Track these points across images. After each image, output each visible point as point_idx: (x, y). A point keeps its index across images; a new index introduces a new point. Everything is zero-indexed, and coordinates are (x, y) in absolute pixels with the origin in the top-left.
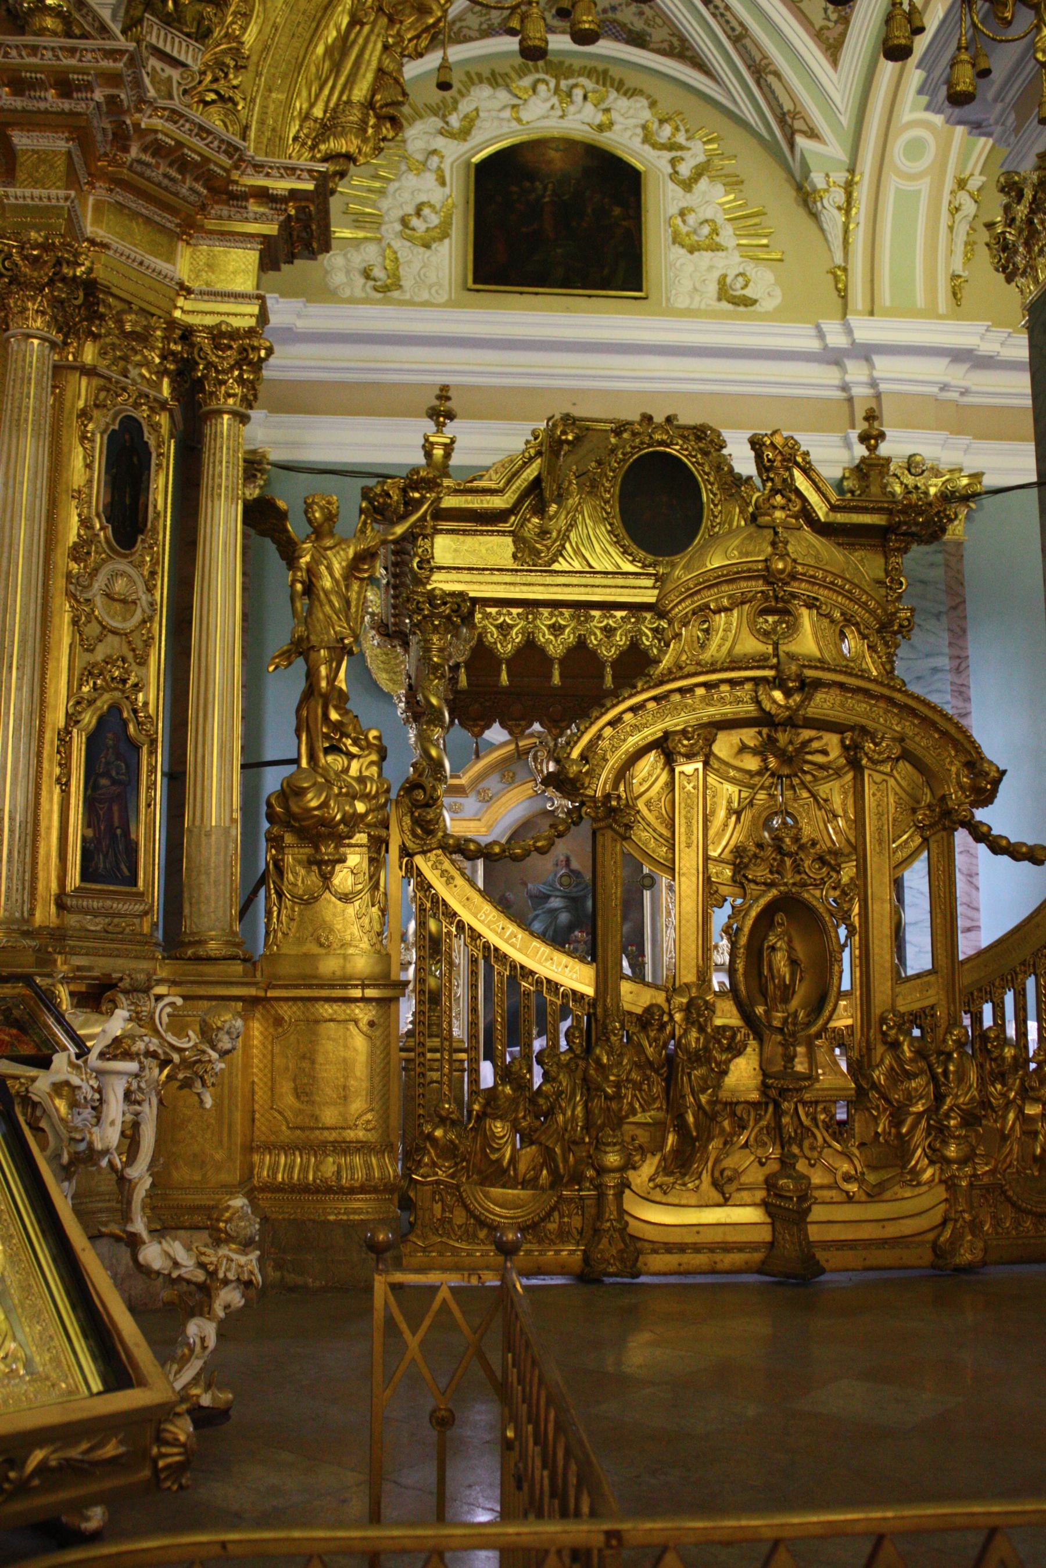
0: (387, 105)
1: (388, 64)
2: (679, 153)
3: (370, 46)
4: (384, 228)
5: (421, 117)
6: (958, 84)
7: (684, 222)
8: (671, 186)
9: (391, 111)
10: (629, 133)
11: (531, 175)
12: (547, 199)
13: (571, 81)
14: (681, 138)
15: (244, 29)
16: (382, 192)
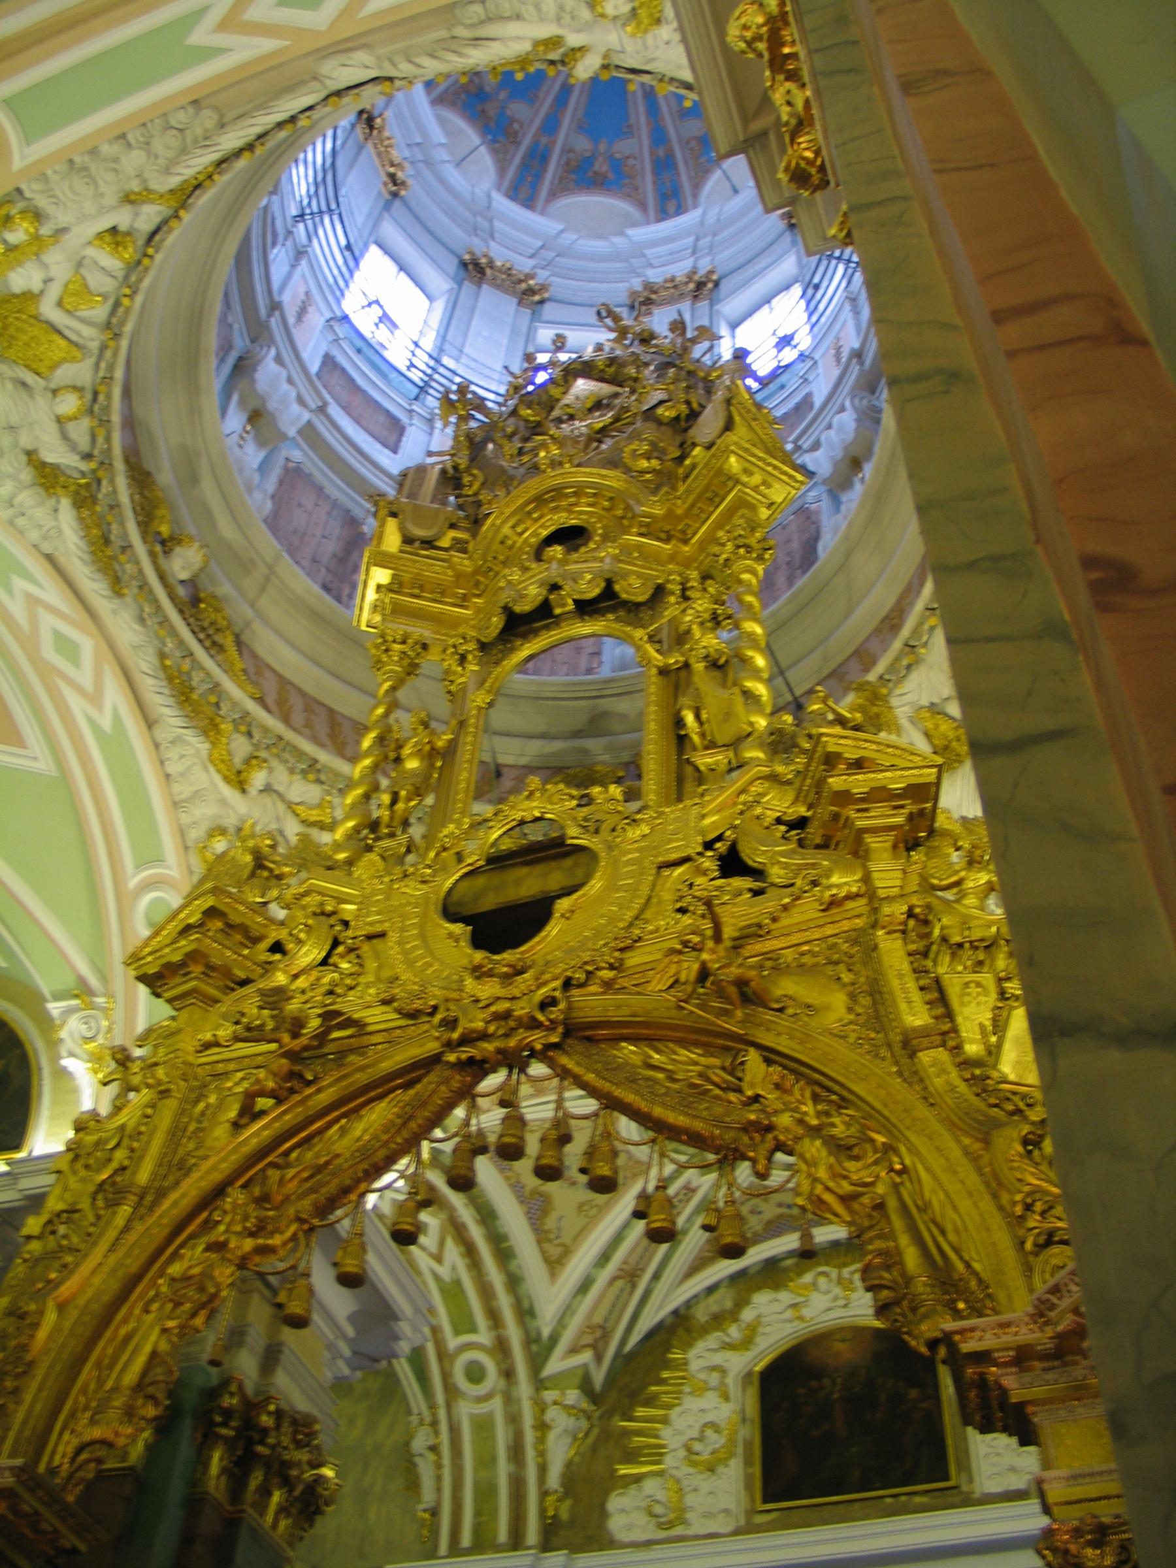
11: (815, 1373)
15: (32, 1337)
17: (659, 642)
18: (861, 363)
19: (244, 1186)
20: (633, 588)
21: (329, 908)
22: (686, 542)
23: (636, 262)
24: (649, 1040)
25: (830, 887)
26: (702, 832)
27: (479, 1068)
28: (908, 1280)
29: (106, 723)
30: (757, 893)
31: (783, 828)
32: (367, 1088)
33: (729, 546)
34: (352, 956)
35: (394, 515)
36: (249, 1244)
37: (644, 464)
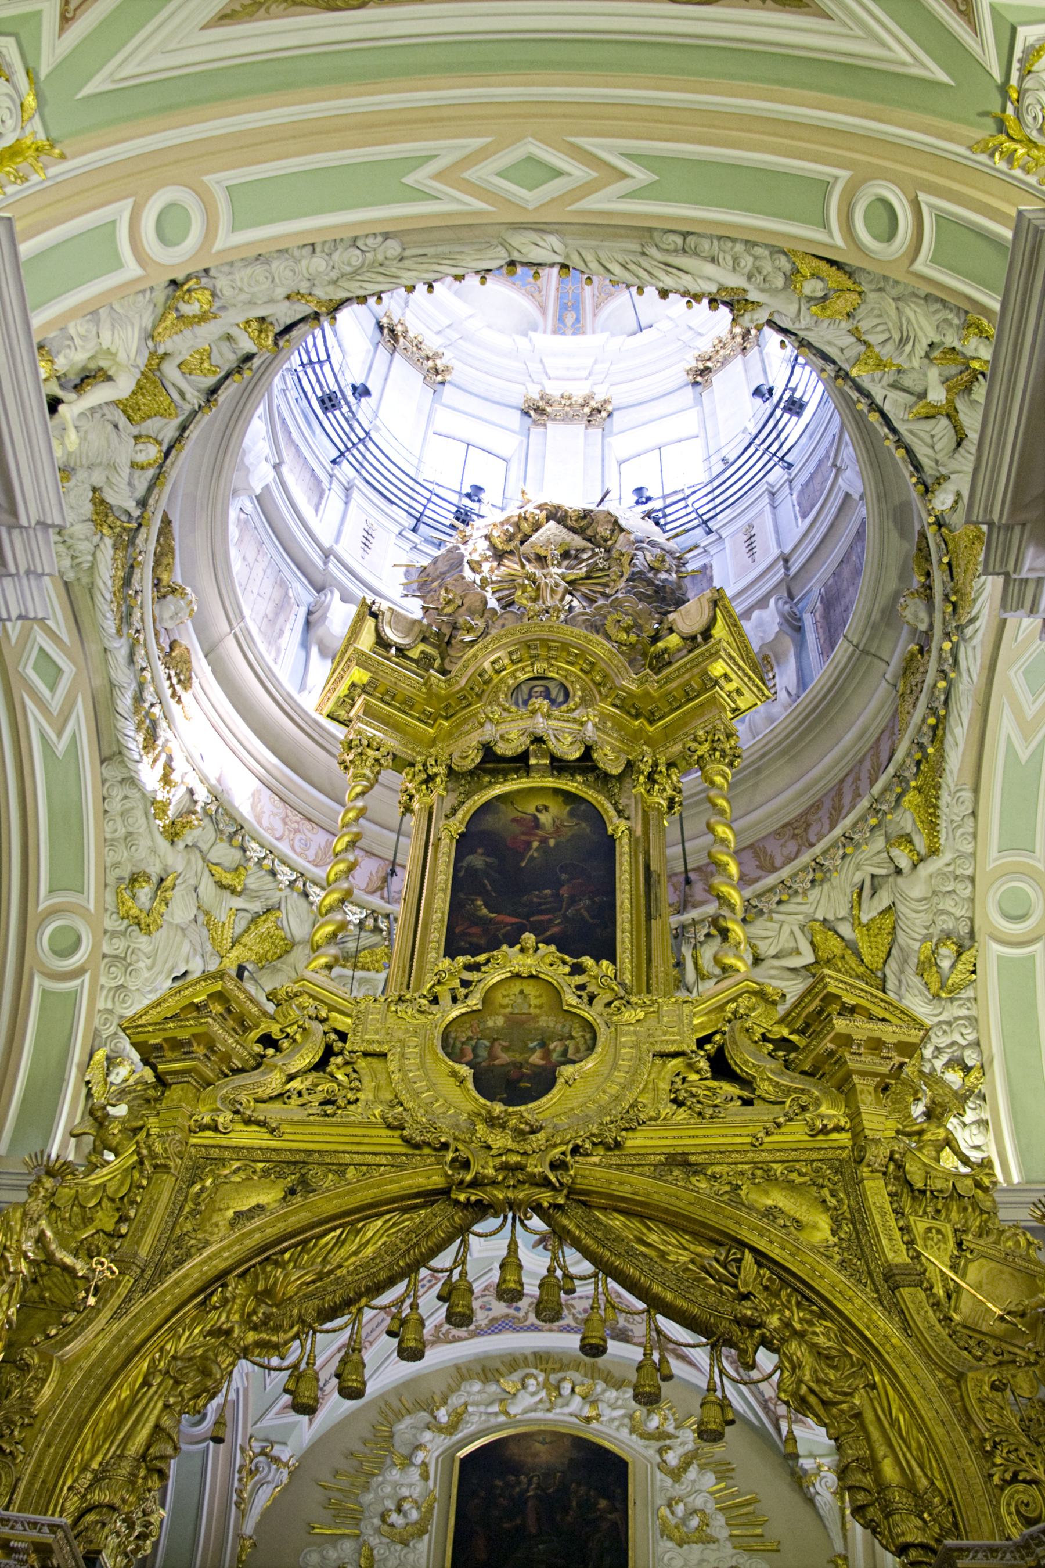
0: (156, 1458)
1: (166, 1422)
2: (668, 1442)
3: (152, 1405)
4: (362, 1524)
5: (409, 1412)
6: (708, 1423)
7: (673, 1513)
8: (659, 1475)
9: (158, 1464)
10: (616, 1423)
11: (515, 1468)
12: (531, 1493)
13: (561, 1375)
14: (670, 1428)
15: (38, 1392)
16: (366, 1488)
17: (628, 819)
18: (787, 569)
19: (242, 1275)
20: (609, 760)
21: (323, 1014)
22: (651, 722)
23: (534, 367)
24: (642, 1217)
25: (822, 1117)
26: (694, 1030)
27: (482, 1209)
28: (882, 1487)
29: (61, 746)
30: (747, 1102)
31: (770, 1046)
32: (371, 1206)
33: (706, 746)
34: (349, 1069)
35: (374, 615)
36: (251, 1337)
37: (624, 636)
